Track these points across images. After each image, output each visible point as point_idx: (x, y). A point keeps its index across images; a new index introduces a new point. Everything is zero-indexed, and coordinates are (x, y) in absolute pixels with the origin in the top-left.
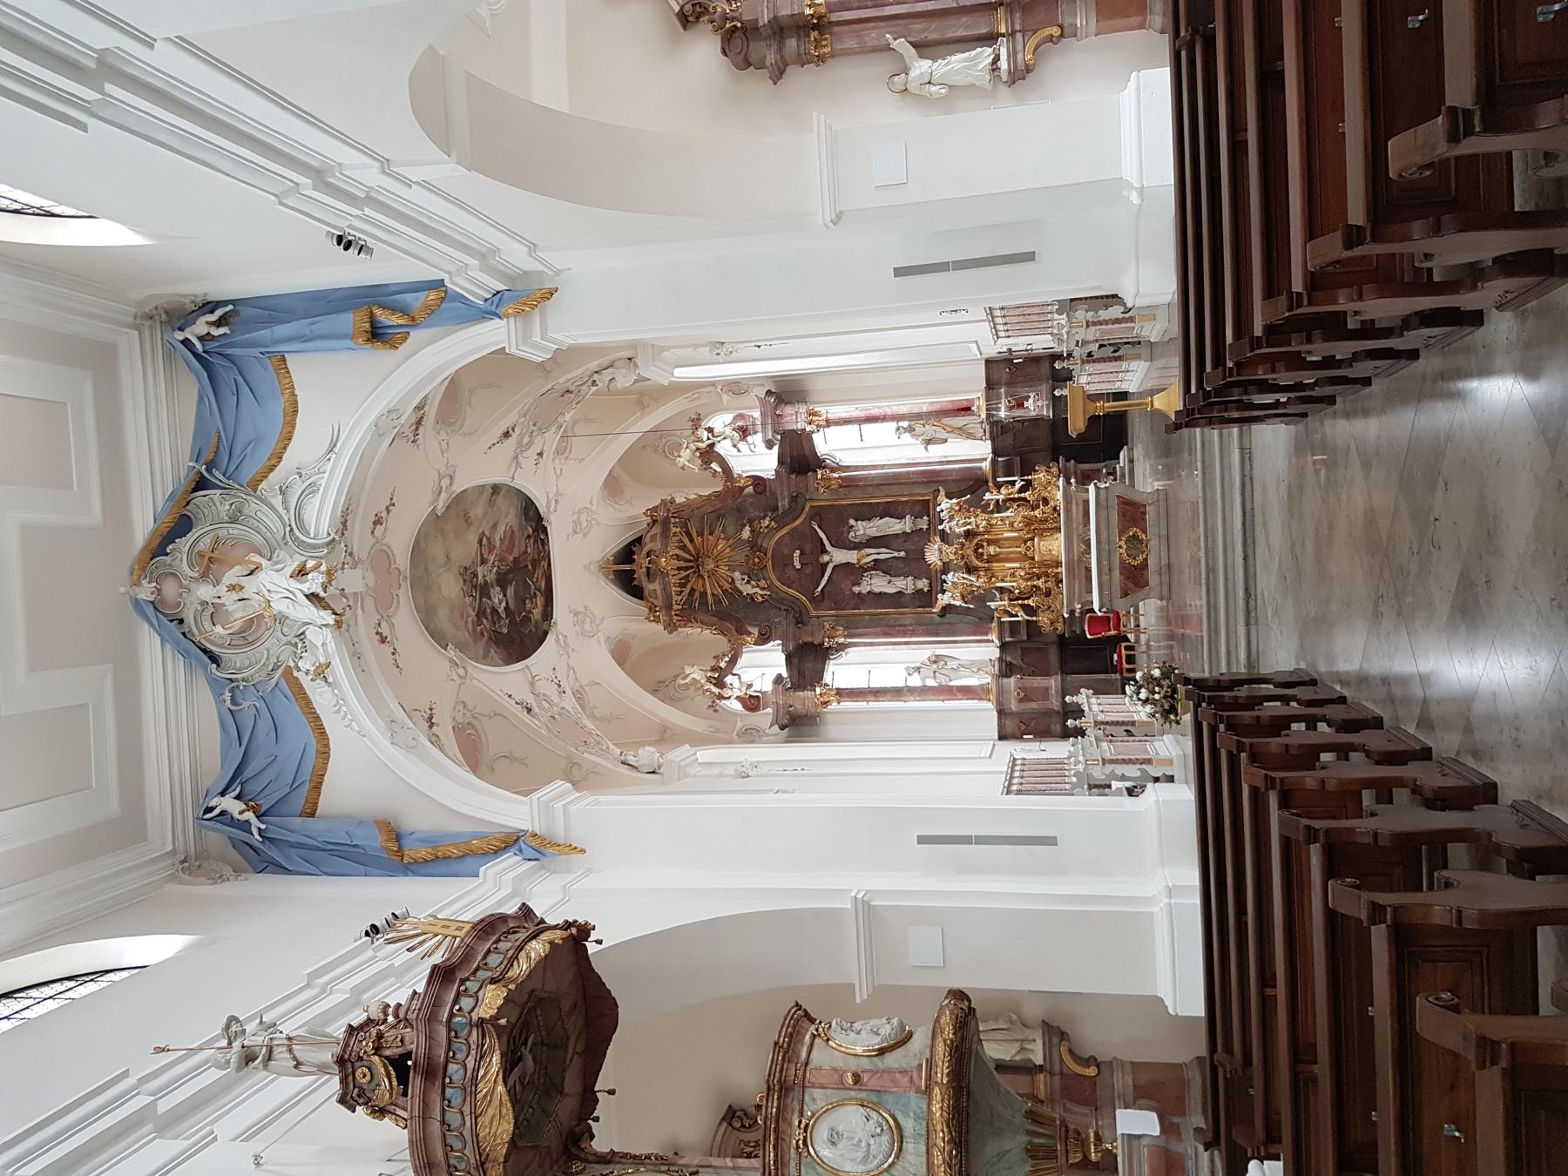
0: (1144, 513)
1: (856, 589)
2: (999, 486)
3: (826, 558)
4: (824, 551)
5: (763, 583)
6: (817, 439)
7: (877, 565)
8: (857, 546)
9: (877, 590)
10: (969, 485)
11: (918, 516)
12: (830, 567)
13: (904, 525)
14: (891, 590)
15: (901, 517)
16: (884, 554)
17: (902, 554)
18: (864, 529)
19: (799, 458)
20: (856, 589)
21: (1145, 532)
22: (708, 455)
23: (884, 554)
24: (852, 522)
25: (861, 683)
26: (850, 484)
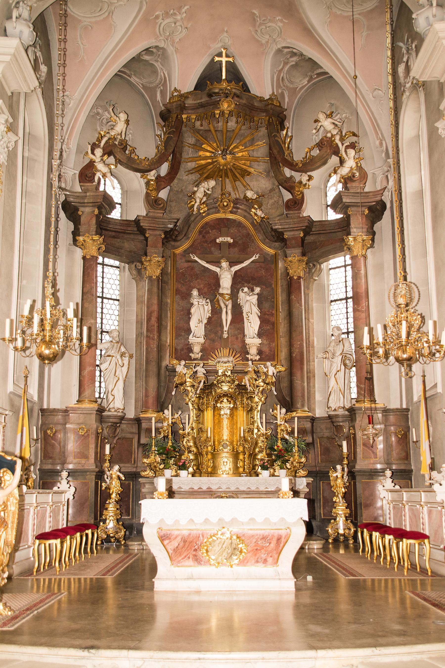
0: (265, 561)
1: (195, 293)
2: (290, 421)
3: (224, 264)
4: (232, 264)
5: (204, 209)
6: (337, 261)
7: (216, 312)
8: (234, 295)
9: (193, 311)
10: (288, 395)
11: (260, 352)
12: (217, 270)
13: (253, 342)
14: (193, 324)
15: (260, 335)
16: (227, 318)
17: (225, 336)
18: (249, 301)
19: (321, 241)
20: (195, 293)
21: (242, 563)
22: (328, 147)
23: (227, 318)
24: (257, 290)
25: (115, 301)
26: (292, 286)
